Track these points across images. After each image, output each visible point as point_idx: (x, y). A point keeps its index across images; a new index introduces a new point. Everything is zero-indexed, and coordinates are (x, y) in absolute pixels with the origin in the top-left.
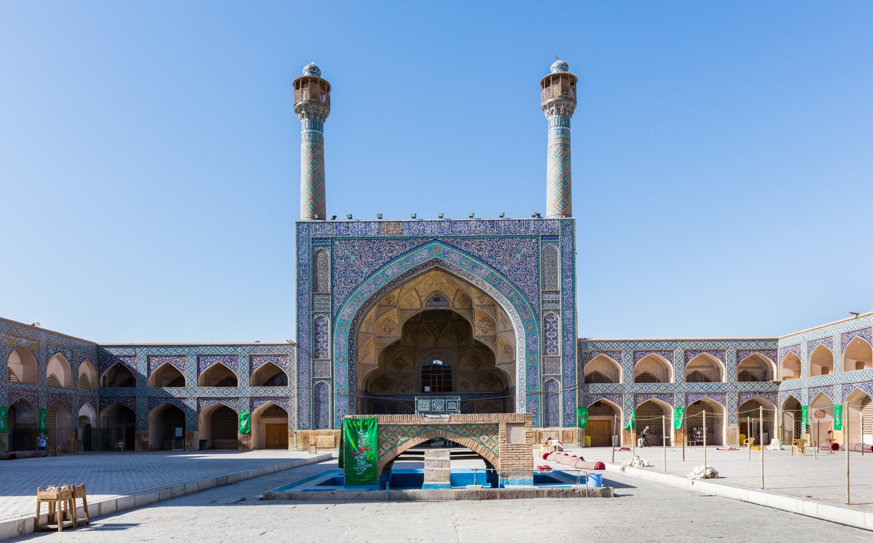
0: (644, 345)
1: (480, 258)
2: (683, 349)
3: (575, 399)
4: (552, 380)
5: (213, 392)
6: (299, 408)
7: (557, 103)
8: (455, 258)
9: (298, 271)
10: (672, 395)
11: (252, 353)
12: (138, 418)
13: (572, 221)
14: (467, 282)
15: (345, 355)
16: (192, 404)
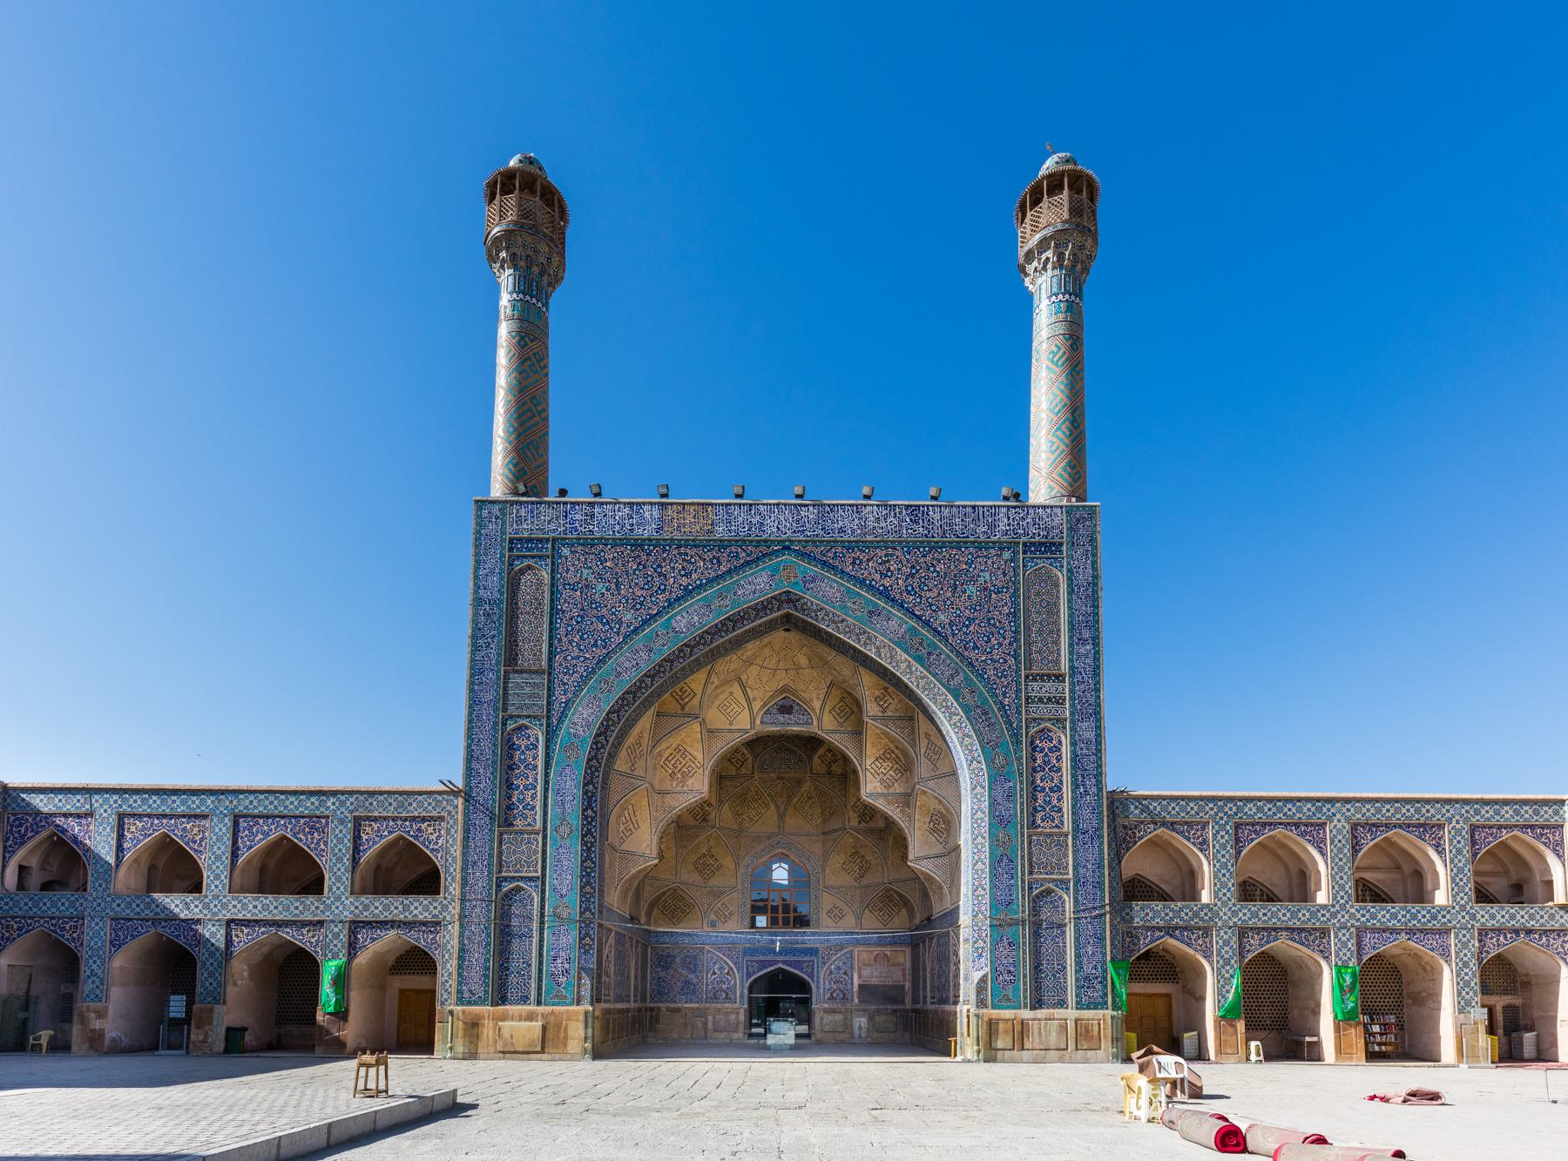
0: (1260, 809)
1: (885, 594)
2: (1348, 819)
4: (1049, 892)
5: (265, 907)
6: (462, 950)
7: (1057, 240)
8: (830, 592)
9: (476, 615)
10: (1324, 932)
11: (361, 813)
12: (84, 971)
15: (575, 820)
16: (214, 933)
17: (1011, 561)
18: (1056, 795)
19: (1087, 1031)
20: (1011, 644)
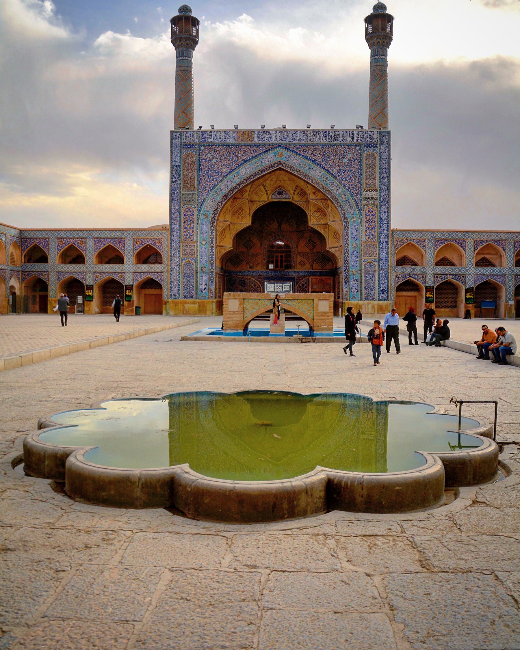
0: (443, 235)
1: (314, 162)
3: (387, 278)
5: (106, 268)
6: (171, 282)
12: (50, 288)
13: (388, 133)
14: (304, 180)
15: (208, 239)
17: (359, 150)
18: (373, 230)
19: (381, 308)
20: (359, 179)
